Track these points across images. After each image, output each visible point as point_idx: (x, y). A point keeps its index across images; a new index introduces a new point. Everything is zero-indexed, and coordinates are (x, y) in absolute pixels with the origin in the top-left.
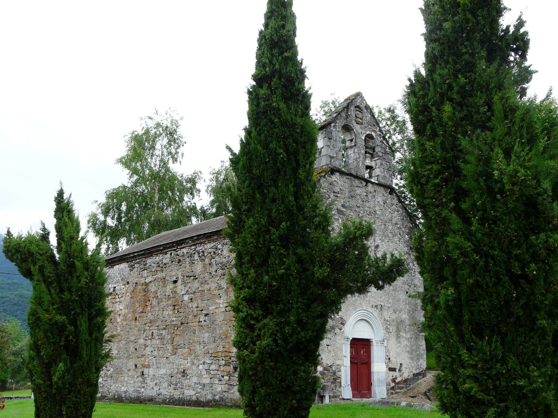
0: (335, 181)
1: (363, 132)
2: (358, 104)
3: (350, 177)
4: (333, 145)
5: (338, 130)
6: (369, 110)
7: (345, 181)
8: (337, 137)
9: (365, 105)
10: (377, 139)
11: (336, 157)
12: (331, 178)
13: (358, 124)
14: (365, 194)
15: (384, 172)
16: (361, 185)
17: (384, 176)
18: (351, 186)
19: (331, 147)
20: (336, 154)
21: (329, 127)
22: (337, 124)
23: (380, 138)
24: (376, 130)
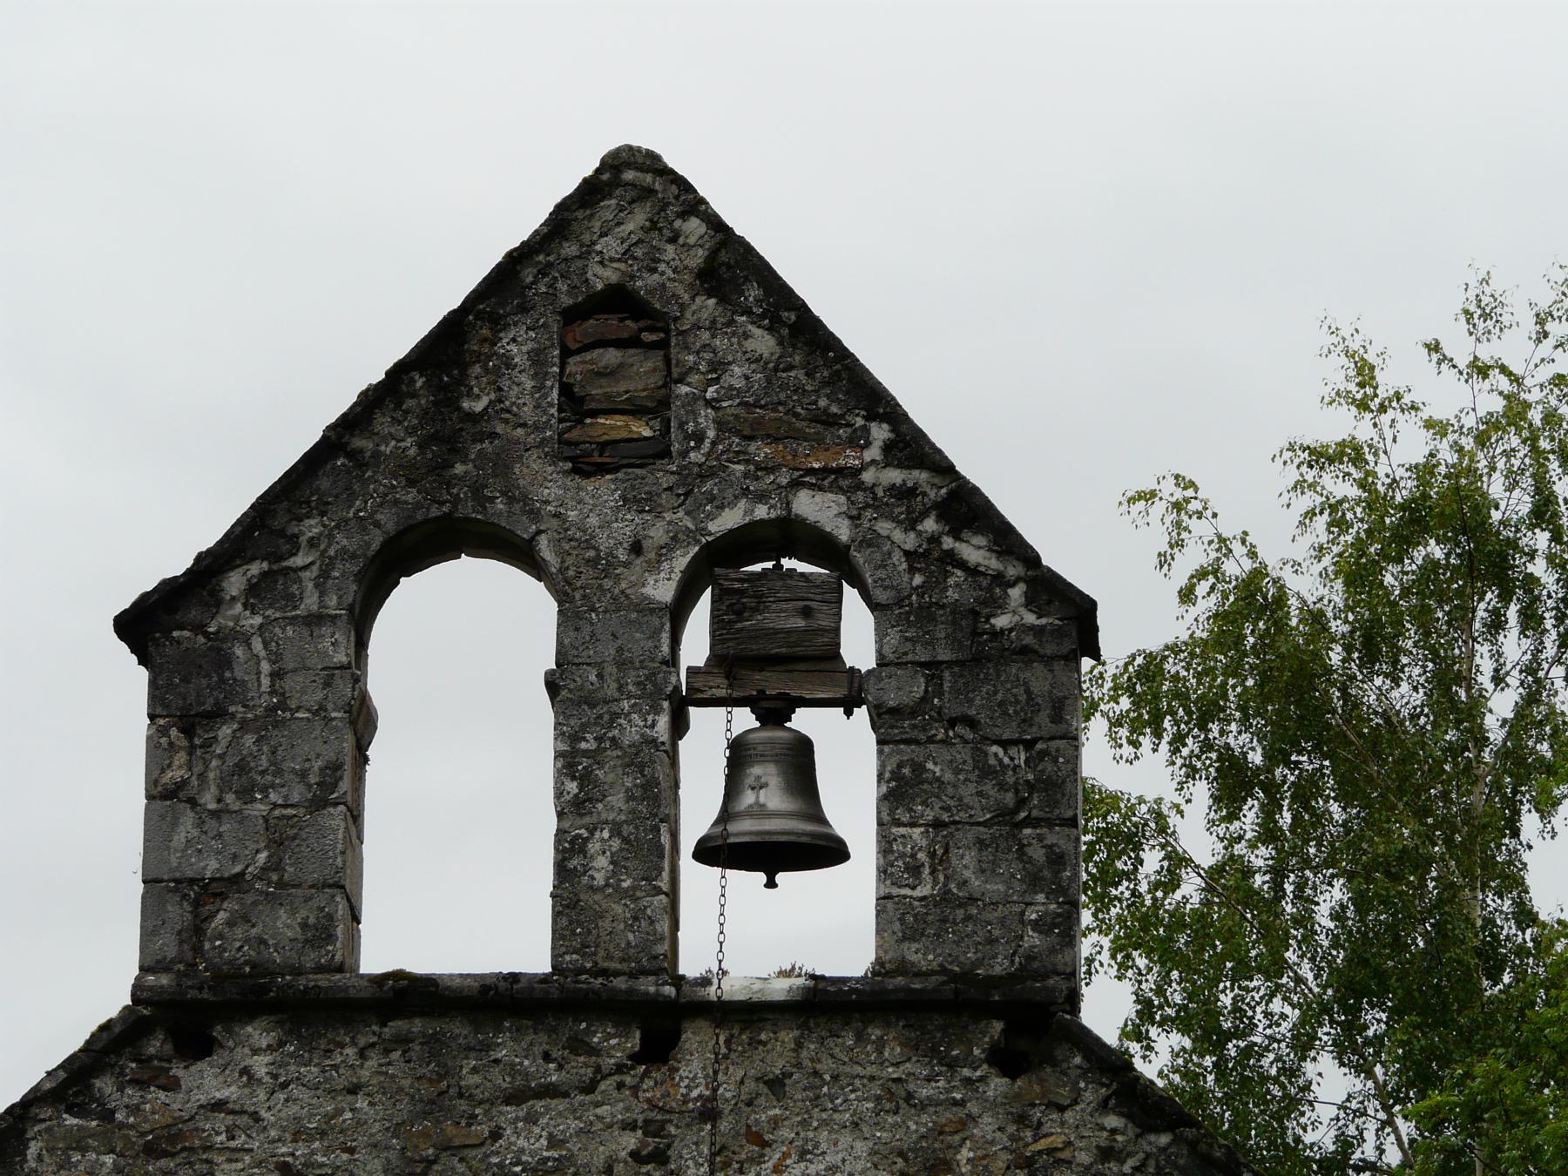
0: (218, 1106)
1: (658, 533)
2: (601, 276)
3: (417, 1025)
4: (242, 768)
5: (310, 602)
6: (753, 293)
7: (341, 1080)
8: (291, 683)
9: (697, 258)
10: (871, 541)
11: (274, 865)
12: (172, 1086)
13: (602, 470)
14: (631, 1141)
15: (939, 861)
16: (581, 1067)
17: (944, 899)
18: (432, 1107)
19: (209, 800)
20: (277, 844)
21: (194, 614)
22: (299, 561)
23: (911, 524)
24: (850, 459)
